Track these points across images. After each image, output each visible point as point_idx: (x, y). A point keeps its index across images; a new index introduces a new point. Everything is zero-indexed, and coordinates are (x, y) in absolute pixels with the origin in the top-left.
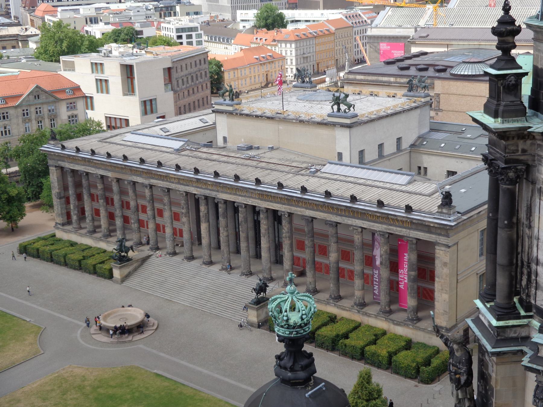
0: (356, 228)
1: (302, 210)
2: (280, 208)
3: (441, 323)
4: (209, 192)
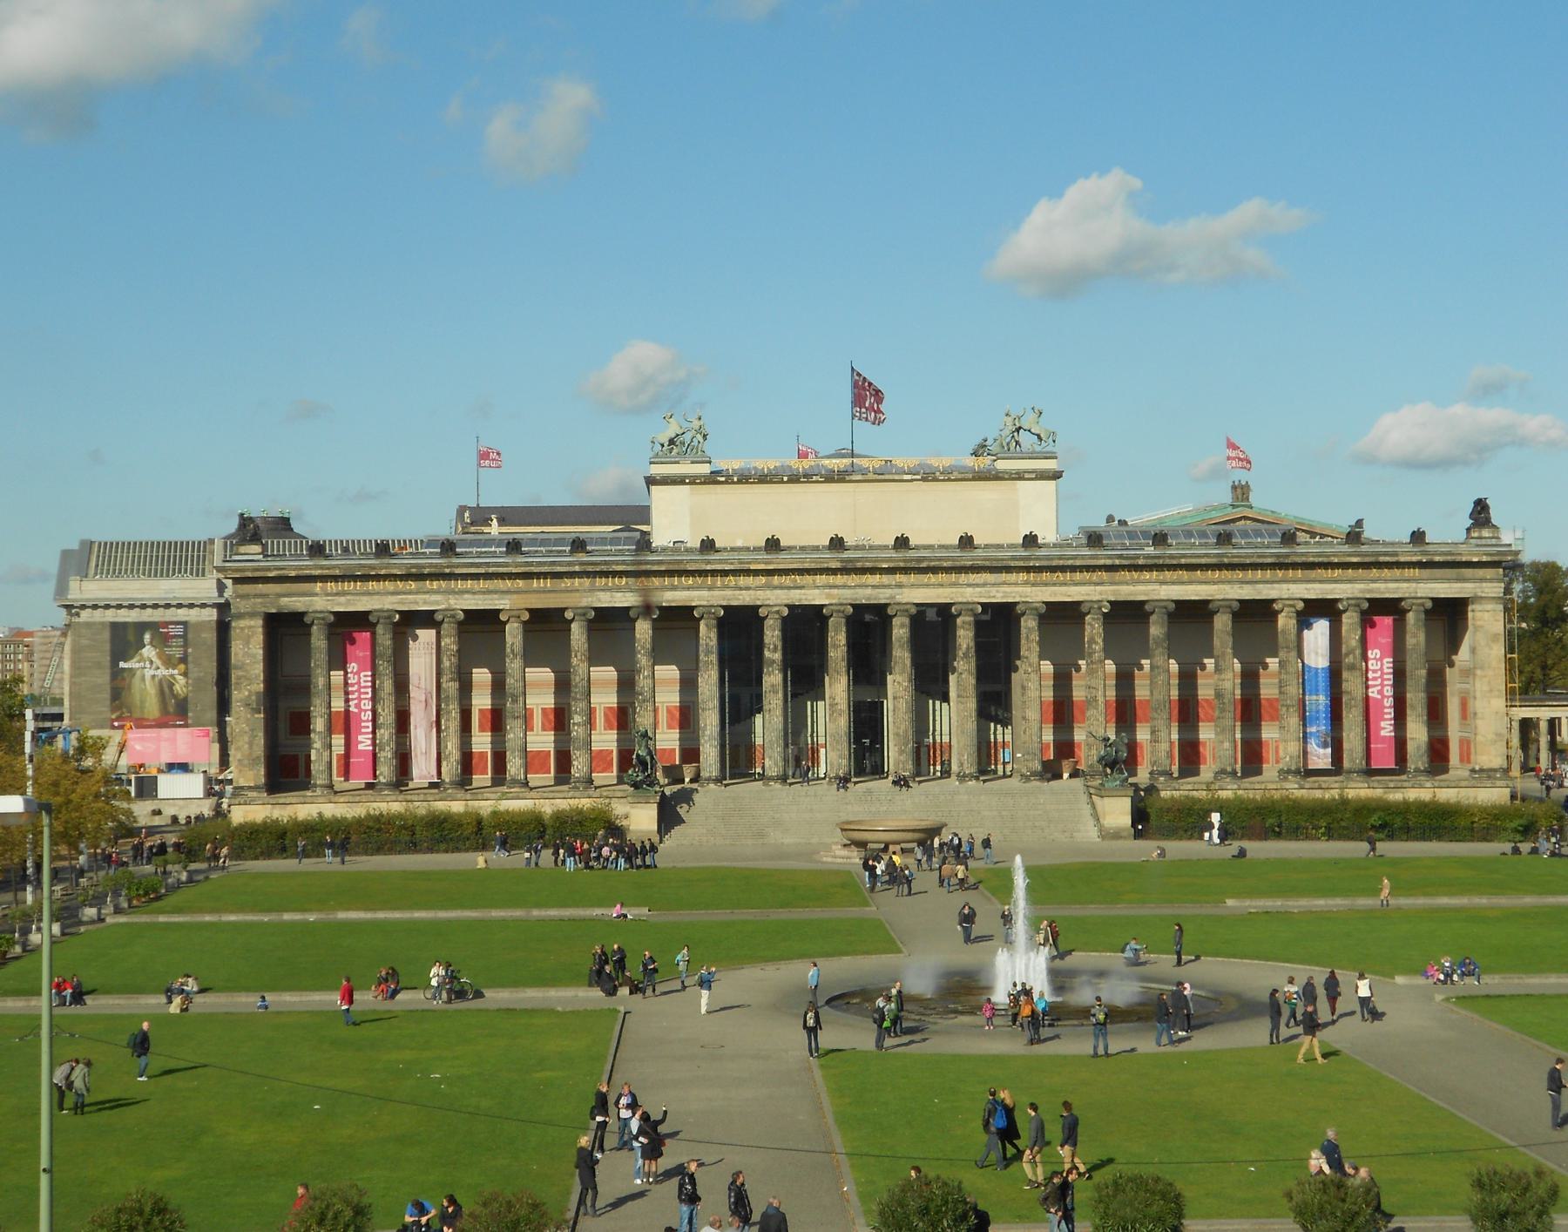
0: (1291, 602)
1: (1150, 587)
3: (1491, 761)
4: (869, 591)
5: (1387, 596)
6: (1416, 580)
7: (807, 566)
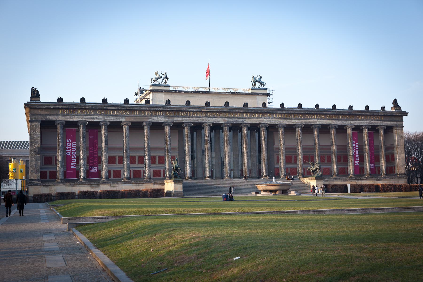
0: (351, 126)
2: (298, 122)
3: (402, 171)
4: (236, 119)
5: (375, 125)
6: (383, 121)
7: (219, 110)
